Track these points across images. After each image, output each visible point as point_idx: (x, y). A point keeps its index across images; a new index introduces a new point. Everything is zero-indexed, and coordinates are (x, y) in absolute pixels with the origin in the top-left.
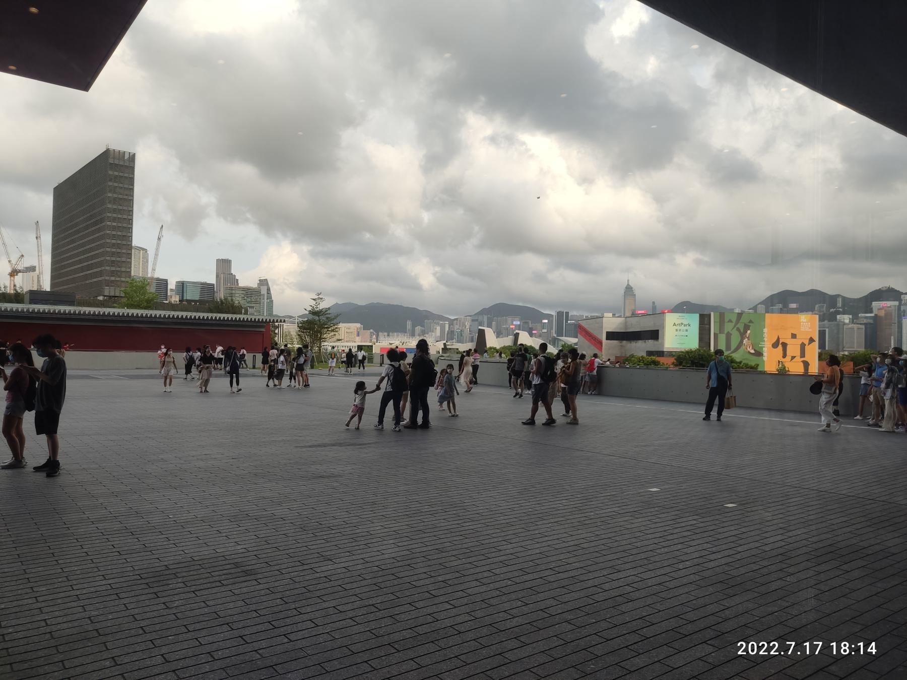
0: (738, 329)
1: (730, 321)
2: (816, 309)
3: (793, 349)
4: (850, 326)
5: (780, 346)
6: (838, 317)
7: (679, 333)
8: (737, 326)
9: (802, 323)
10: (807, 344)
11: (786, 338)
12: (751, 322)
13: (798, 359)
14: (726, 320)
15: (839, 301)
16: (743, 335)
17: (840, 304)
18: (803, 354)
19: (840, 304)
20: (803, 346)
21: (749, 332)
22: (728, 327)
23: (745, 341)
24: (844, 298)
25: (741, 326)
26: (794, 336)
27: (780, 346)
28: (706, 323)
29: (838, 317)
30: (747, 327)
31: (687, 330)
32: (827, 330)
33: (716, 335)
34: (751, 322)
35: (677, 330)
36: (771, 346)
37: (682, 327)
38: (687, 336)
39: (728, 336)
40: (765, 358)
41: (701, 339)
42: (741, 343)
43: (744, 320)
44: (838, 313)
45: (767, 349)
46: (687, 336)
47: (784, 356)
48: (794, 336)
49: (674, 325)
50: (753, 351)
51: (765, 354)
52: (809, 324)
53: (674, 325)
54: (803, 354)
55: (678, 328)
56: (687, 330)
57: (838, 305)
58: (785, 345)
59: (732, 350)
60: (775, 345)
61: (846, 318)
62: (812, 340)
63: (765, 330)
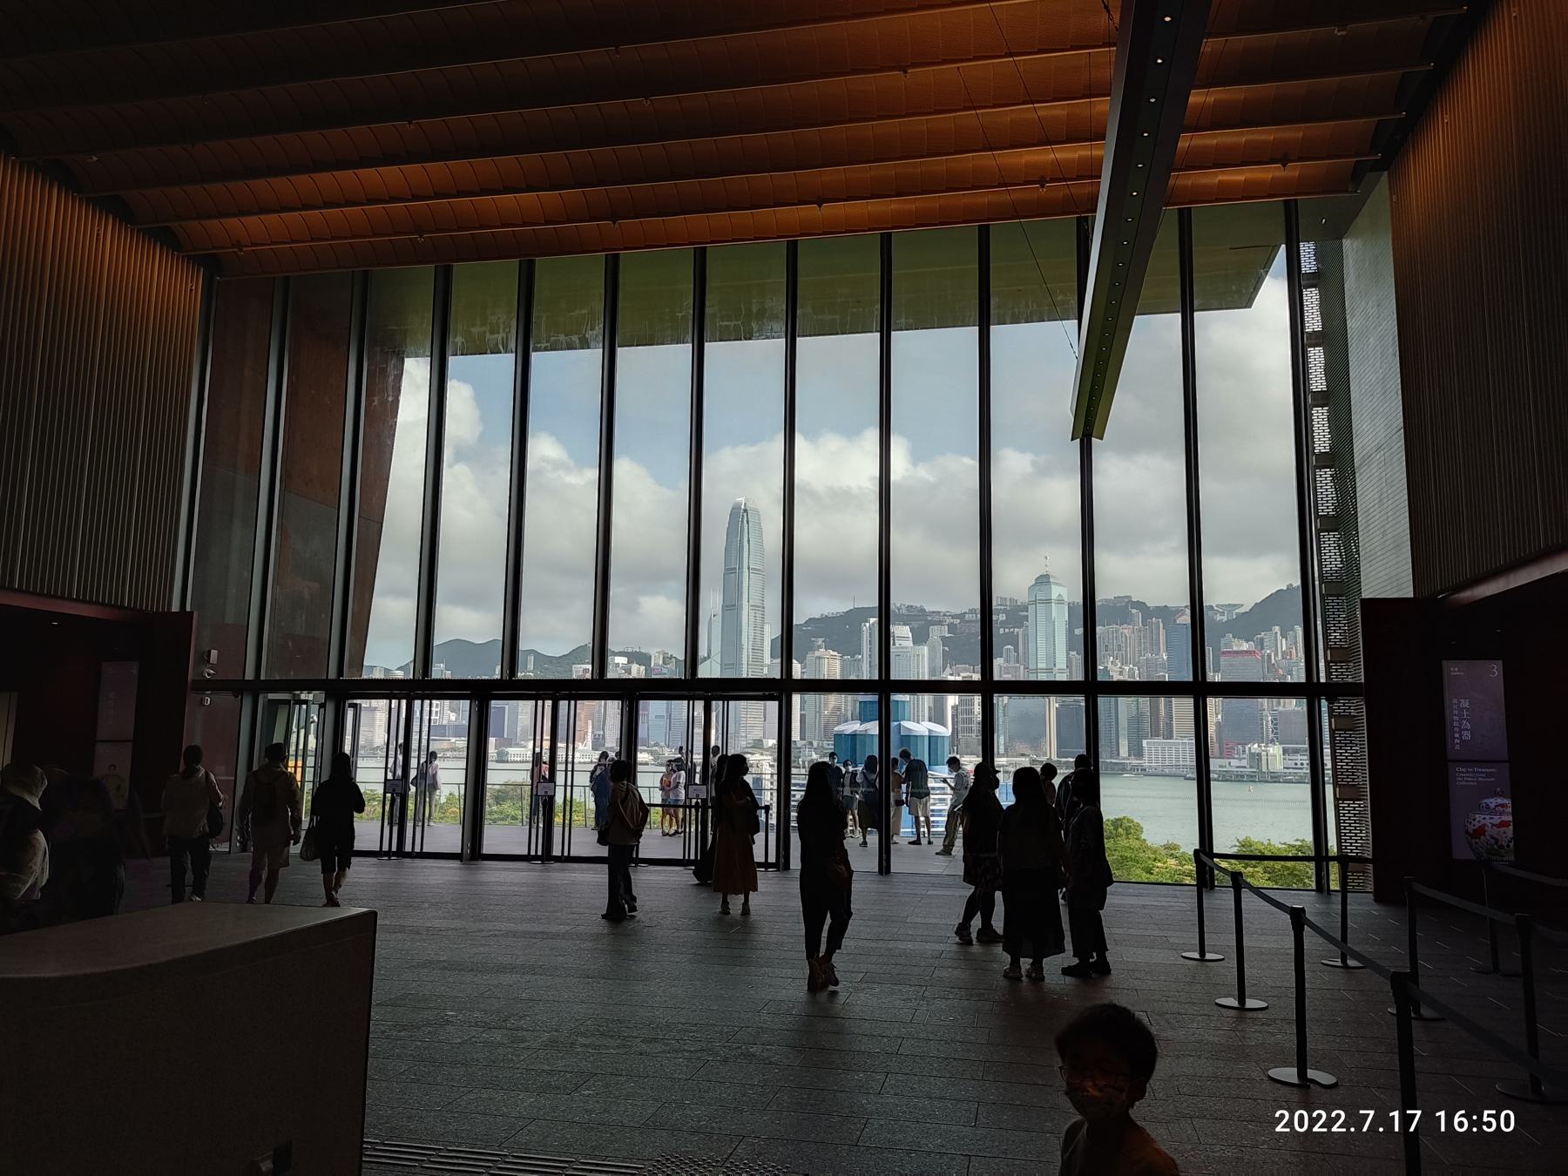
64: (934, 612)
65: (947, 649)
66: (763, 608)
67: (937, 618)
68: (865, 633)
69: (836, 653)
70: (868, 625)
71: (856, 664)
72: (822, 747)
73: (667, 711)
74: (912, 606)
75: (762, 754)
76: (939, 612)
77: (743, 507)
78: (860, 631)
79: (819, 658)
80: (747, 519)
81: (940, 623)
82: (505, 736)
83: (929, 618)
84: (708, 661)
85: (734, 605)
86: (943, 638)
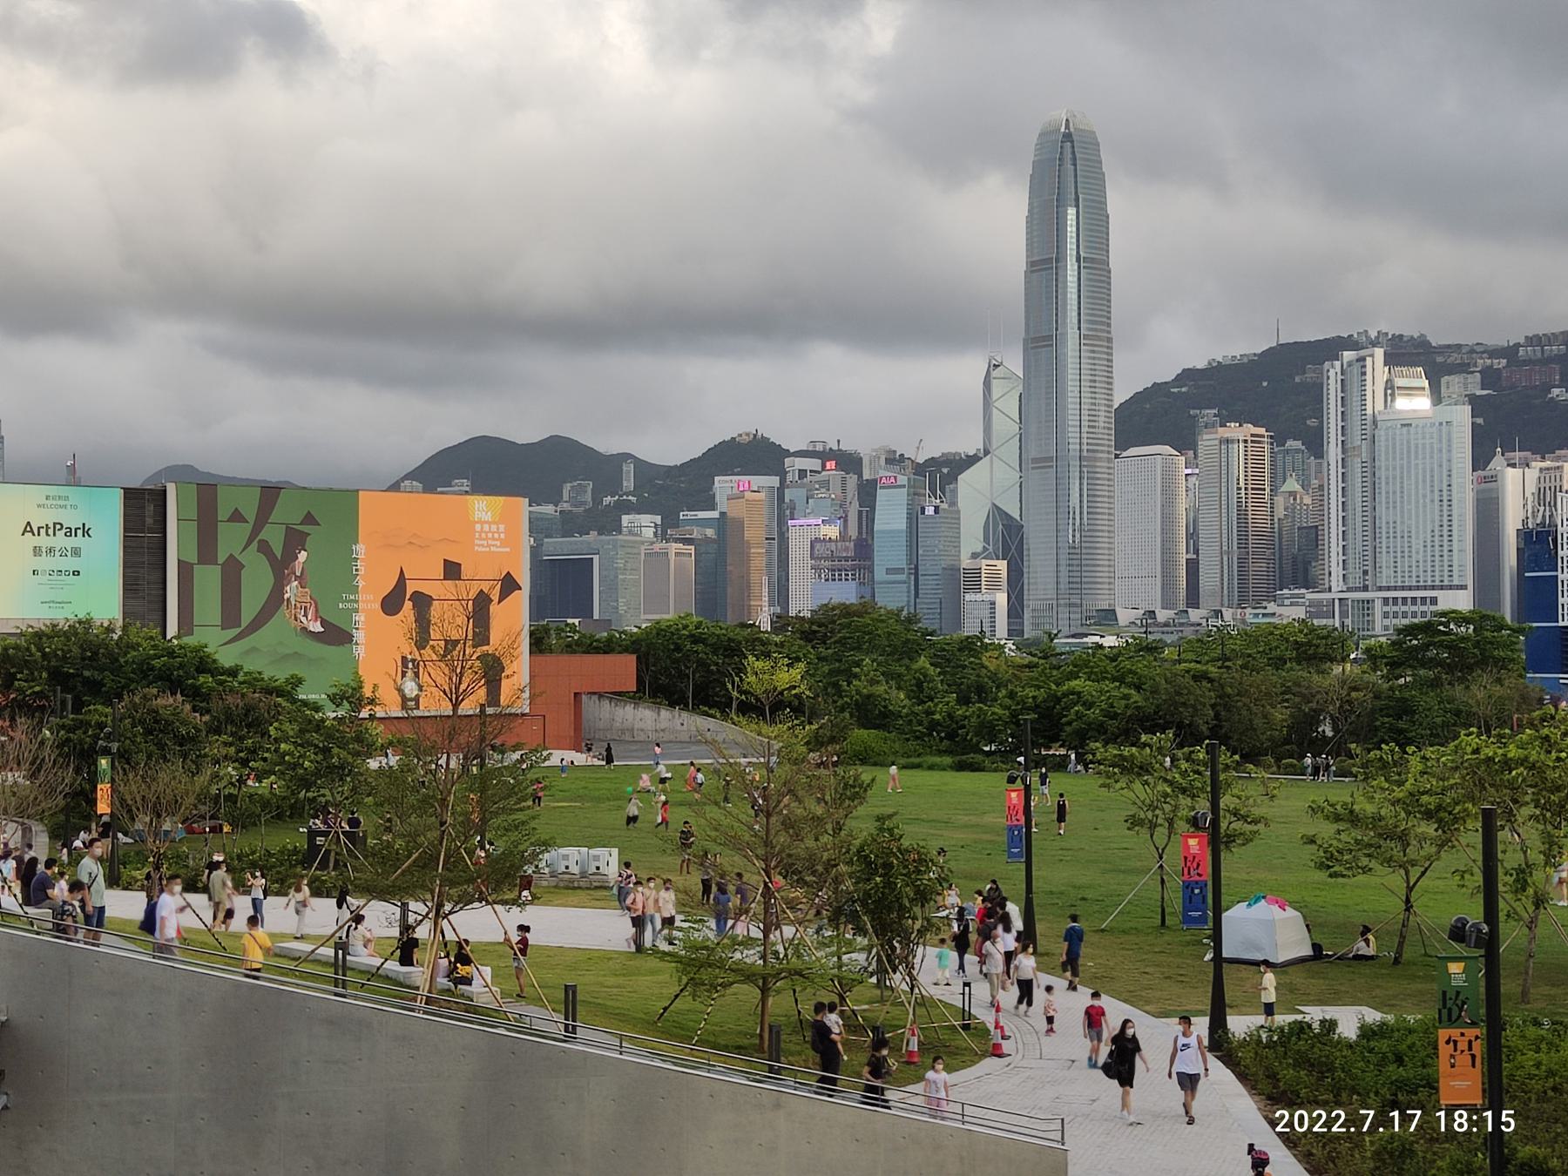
1: (237, 517)
2: (566, 497)
4: (658, 547)
5: (408, 605)
6: (625, 519)
8: (262, 536)
9: (478, 527)
10: (495, 596)
11: (425, 577)
14: (223, 513)
15: (629, 472)
16: (281, 567)
17: (629, 483)
19: (629, 483)
22: (230, 539)
23: (291, 590)
24: (640, 465)
27: (408, 605)
28: (149, 521)
29: (625, 519)
32: (596, 558)
33: (185, 569)
34: (310, 519)
36: (378, 606)
40: (360, 651)
41: (130, 587)
42: (275, 600)
43: (286, 512)
44: (628, 508)
45: (368, 623)
47: (422, 641)
48: (452, 570)
50: (317, 627)
51: (359, 636)
52: (502, 527)
57: (625, 484)
59: (244, 625)
60: (391, 604)
61: (646, 524)
62: (509, 585)
63: (360, 549)
64: (1449, 346)
66: (1110, 340)
67: (1455, 358)
68: (1331, 381)
69: (1262, 431)
70: (1337, 364)
71: (1289, 459)
72: (1243, 621)
73: (910, 562)
74: (1401, 336)
76: (1459, 346)
77: (1063, 130)
79: (1228, 441)
80: (1073, 153)
81: (1463, 368)
82: (596, 616)
83: (1440, 359)
84: (988, 457)
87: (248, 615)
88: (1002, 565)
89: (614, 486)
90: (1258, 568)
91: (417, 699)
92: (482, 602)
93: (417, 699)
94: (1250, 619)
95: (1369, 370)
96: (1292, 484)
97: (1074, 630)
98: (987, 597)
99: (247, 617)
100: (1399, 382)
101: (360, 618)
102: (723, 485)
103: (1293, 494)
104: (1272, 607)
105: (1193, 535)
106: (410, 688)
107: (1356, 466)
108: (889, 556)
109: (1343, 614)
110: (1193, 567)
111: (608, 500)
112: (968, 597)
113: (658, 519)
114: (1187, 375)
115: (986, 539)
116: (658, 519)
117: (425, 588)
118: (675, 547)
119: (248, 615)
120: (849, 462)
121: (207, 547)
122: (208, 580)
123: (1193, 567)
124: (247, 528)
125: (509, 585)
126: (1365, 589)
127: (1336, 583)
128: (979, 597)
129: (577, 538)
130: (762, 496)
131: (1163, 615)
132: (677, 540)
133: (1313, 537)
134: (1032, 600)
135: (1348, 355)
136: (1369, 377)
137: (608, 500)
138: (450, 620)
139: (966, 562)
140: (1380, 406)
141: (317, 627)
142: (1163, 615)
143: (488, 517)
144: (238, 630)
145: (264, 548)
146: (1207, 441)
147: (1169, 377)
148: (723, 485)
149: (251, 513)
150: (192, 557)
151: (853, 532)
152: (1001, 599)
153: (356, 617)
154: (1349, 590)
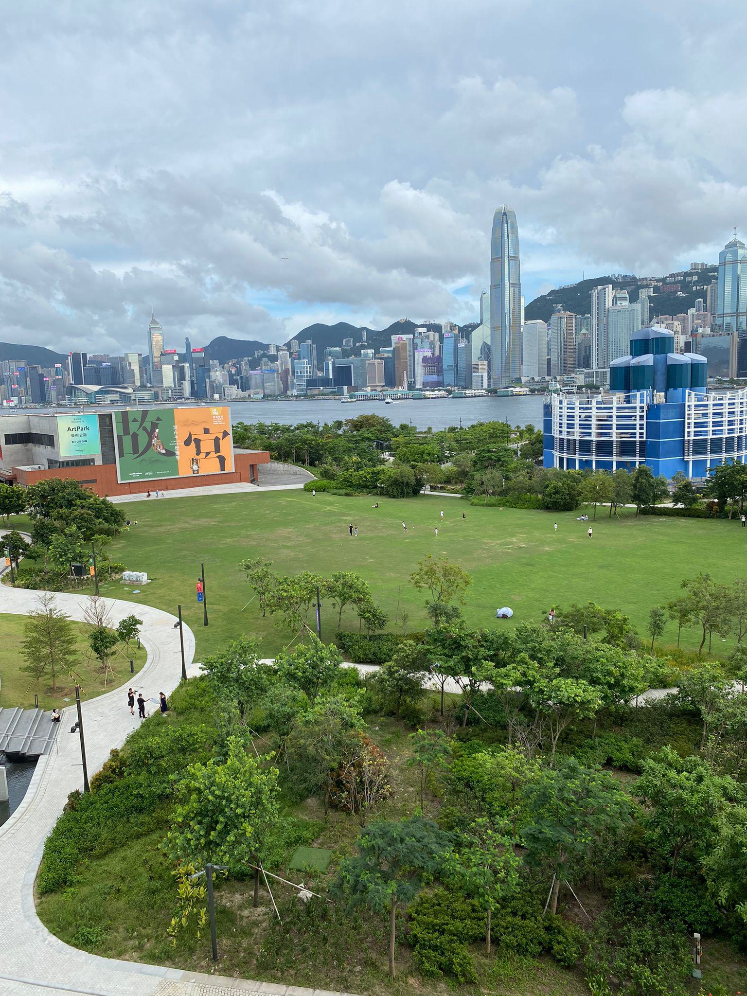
0: (145, 429)
3: (207, 445)
5: (193, 442)
7: (75, 439)
10: (221, 437)
12: (158, 419)
13: (213, 455)
16: (151, 434)
18: (217, 449)
20: (217, 440)
21: (157, 430)
22: (133, 427)
23: (154, 441)
25: (147, 424)
26: (206, 431)
27: (193, 442)
30: (154, 426)
31: (85, 435)
35: (73, 436)
37: (79, 432)
38: (86, 441)
39: (135, 437)
41: (103, 444)
42: (149, 444)
46: (86, 441)
47: (198, 452)
49: (69, 429)
50: (164, 452)
53: (69, 429)
54: (217, 449)
55: (74, 432)
56: (85, 435)
58: (198, 442)
59: (140, 452)
60: (187, 443)
62: (225, 434)
65: (652, 305)
66: (520, 285)
69: (572, 314)
75: (521, 387)
78: (590, 296)
85: (499, 285)
86: (650, 297)
87: (141, 449)
88: (486, 363)
89: (360, 339)
90: (570, 361)
91: (198, 471)
92: (217, 440)
93: (198, 471)
94: (566, 379)
95: (607, 292)
96: (584, 331)
97: (505, 386)
98: (480, 374)
99: (141, 450)
100: (617, 296)
101: (177, 448)
102: (394, 338)
103: (584, 334)
104: (573, 375)
105: (549, 350)
106: (195, 467)
107: (602, 325)
108: (448, 361)
109: (597, 377)
110: (549, 361)
111: (358, 344)
112: (474, 374)
113: (373, 351)
114: (552, 293)
115: (481, 354)
116: (373, 351)
117: (199, 437)
118: (377, 361)
119: (141, 450)
120: (436, 328)
121: (126, 431)
122: (127, 441)
123: (549, 361)
124: (138, 424)
125: (225, 434)
126: (604, 368)
127: (594, 366)
128: (477, 374)
129: (346, 359)
130: (407, 342)
131: (537, 379)
132: (378, 359)
133: (588, 348)
134: (493, 377)
135: (600, 287)
136: (607, 295)
137: (358, 344)
138: (207, 445)
139: (473, 363)
140: (610, 304)
141: (164, 452)
142: (537, 379)
143: (217, 414)
144: (138, 455)
145: (145, 429)
146: (554, 318)
147: (546, 294)
148: (394, 338)
149: (139, 419)
150: (122, 434)
151: (437, 353)
152: (485, 375)
153: (176, 448)
154: (599, 368)
